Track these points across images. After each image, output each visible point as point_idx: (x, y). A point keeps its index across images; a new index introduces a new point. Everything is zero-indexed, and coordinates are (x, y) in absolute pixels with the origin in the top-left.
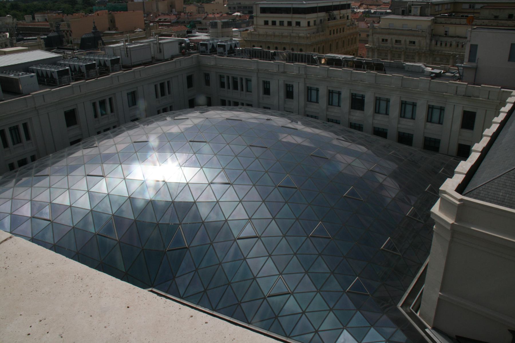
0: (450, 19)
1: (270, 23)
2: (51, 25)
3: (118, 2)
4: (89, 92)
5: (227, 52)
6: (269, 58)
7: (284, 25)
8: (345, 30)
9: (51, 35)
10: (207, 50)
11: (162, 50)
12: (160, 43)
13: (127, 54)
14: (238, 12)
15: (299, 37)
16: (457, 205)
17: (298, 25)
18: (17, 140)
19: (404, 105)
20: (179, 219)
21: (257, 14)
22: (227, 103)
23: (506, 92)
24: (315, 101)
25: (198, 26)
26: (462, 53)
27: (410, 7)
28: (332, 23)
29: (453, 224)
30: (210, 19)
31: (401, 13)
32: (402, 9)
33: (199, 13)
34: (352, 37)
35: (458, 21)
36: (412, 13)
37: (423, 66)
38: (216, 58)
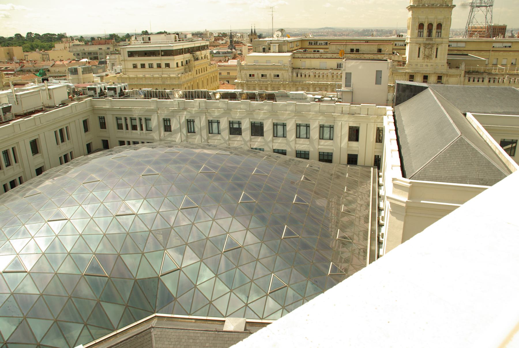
0: (305, 54)
1: (139, 66)
5: (118, 95)
6: (165, 97)
8: (208, 69)
10: (96, 94)
11: (52, 97)
12: (49, 89)
13: (17, 101)
14: (83, 58)
15: (171, 78)
16: (409, 187)
19: (298, 127)
20: (162, 246)
22: (126, 143)
23: (380, 108)
24: (217, 132)
25: (48, 74)
26: (320, 82)
27: (269, 45)
28: (197, 63)
29: (407, 201)
30: (59, 66)
31: (261, 50)
32: (263, 47)
33: (44, 61)
34: (214, 75)
35: (312, 55)
36: (272, 50)
37: (305, 93)
38: (111, 101)
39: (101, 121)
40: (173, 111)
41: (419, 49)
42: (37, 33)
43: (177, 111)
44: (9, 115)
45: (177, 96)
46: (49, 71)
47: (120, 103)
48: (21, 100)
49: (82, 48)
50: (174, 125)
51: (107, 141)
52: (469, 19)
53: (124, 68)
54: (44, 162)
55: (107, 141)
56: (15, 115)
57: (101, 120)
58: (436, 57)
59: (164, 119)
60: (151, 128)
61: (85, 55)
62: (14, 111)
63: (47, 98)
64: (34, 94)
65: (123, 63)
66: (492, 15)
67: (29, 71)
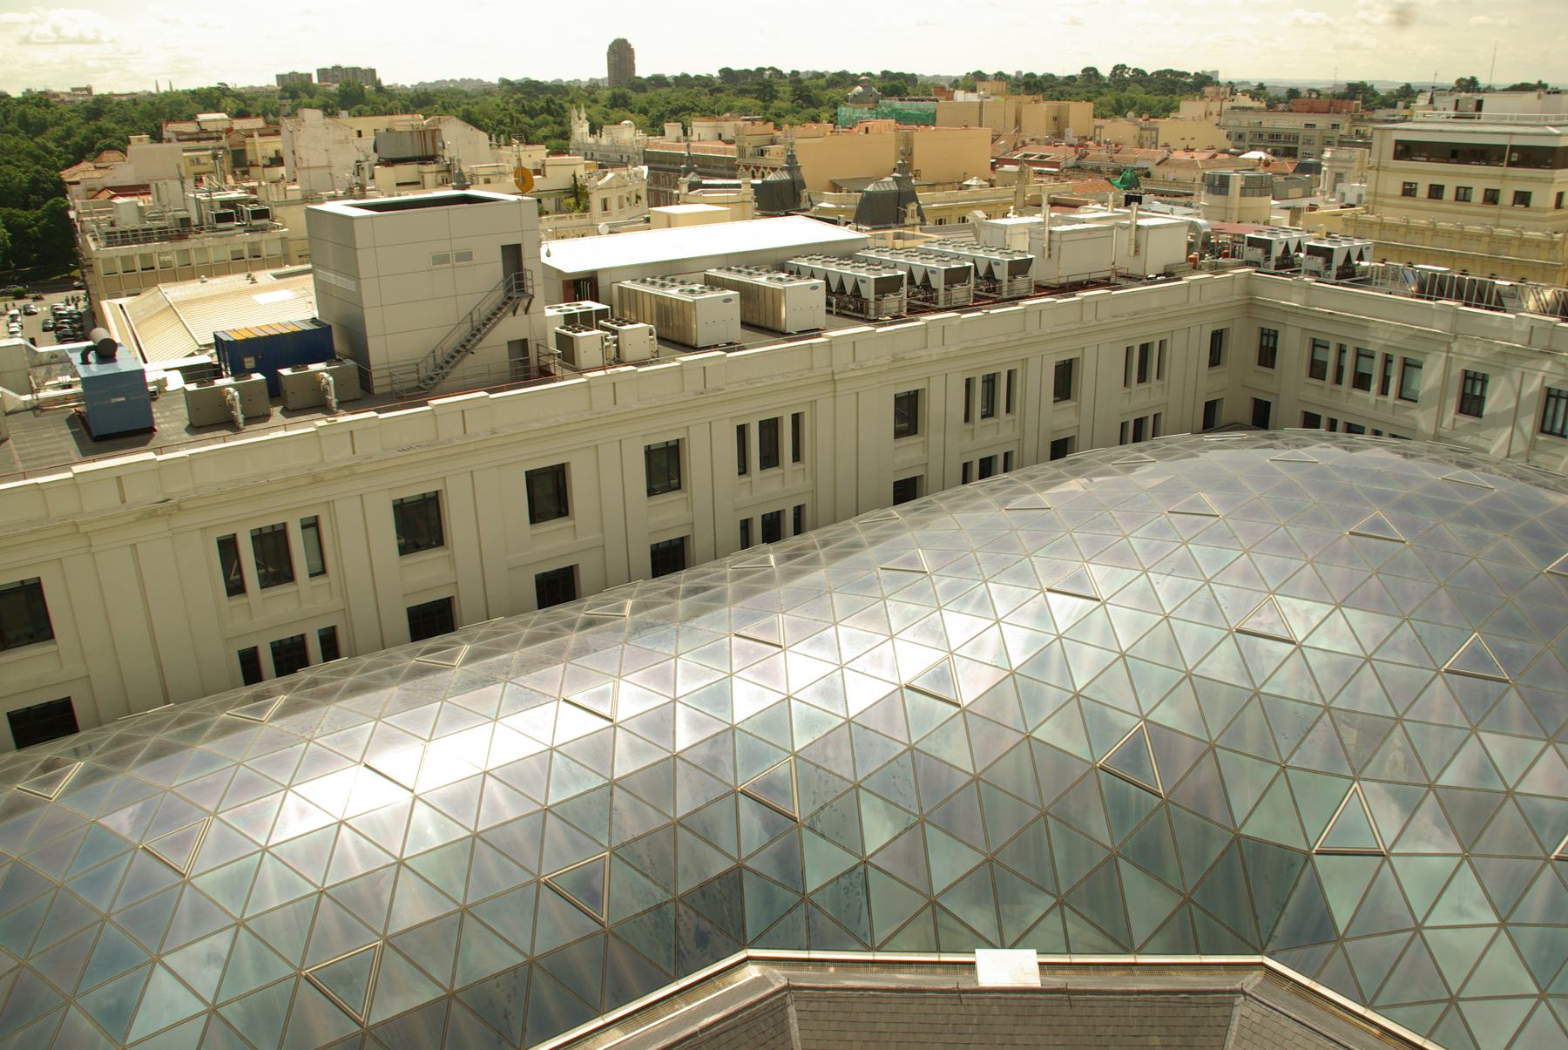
2: (742, 152)
3: (909, 100)
4: (966, 348)
5: (1334, 272)
6: (1489, 302)
7: (1469, 201)
9: (771, 177)
10: (1268, 259)
12: (1138, 227)
13: (1050, 250)
14: (1252, 148)
15: (1524, 242)
17: (1521, 203)
18: (770, 459)
21: (1379, 162)
22: (1324, 422)
30: (1180, 164)
33: (1141, 146)
38: (1309, 287)
39: (1265, 344)
40: (1506, 354)
42: (1140, 68)
43: (1520, 353)
44: (1021, 283)
45: (1531, 304)
46: (1148, 175)
47: (1333, 298)
48: (1059, 248)
49: (1254, 119)
50: (1496, 399)
51: (1268, 404)
53: (1373, 190)
54: (1078, 427)
55: (1268, 404)
56: (1036, 286)
57: (1265, 338)
59: (1466, 372)
60: (1418, 392)
61: (1259, 139)
62: (1035, 274)
63: (1129, 250)
64: (1097, 234)
65: (1372, 175)
67: (1098, 170)
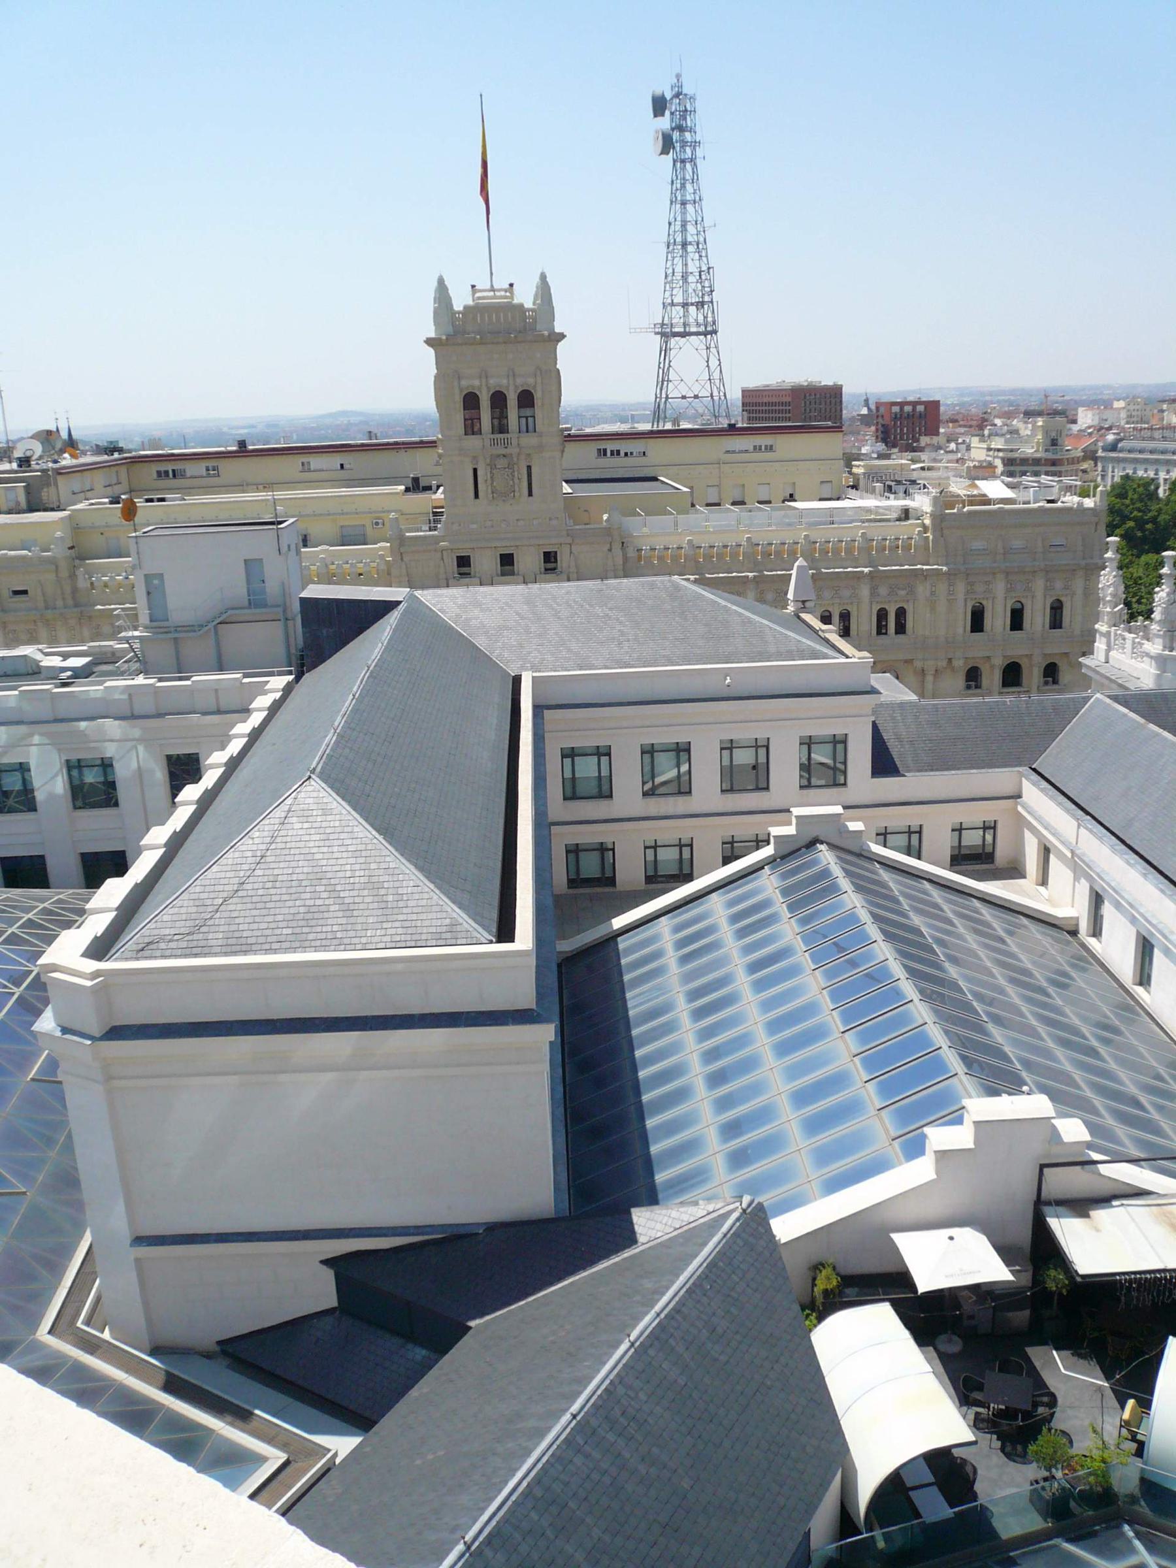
41: (475, 470)
52: (661, 371)
58: (530, 494)
66: (719, 360)
